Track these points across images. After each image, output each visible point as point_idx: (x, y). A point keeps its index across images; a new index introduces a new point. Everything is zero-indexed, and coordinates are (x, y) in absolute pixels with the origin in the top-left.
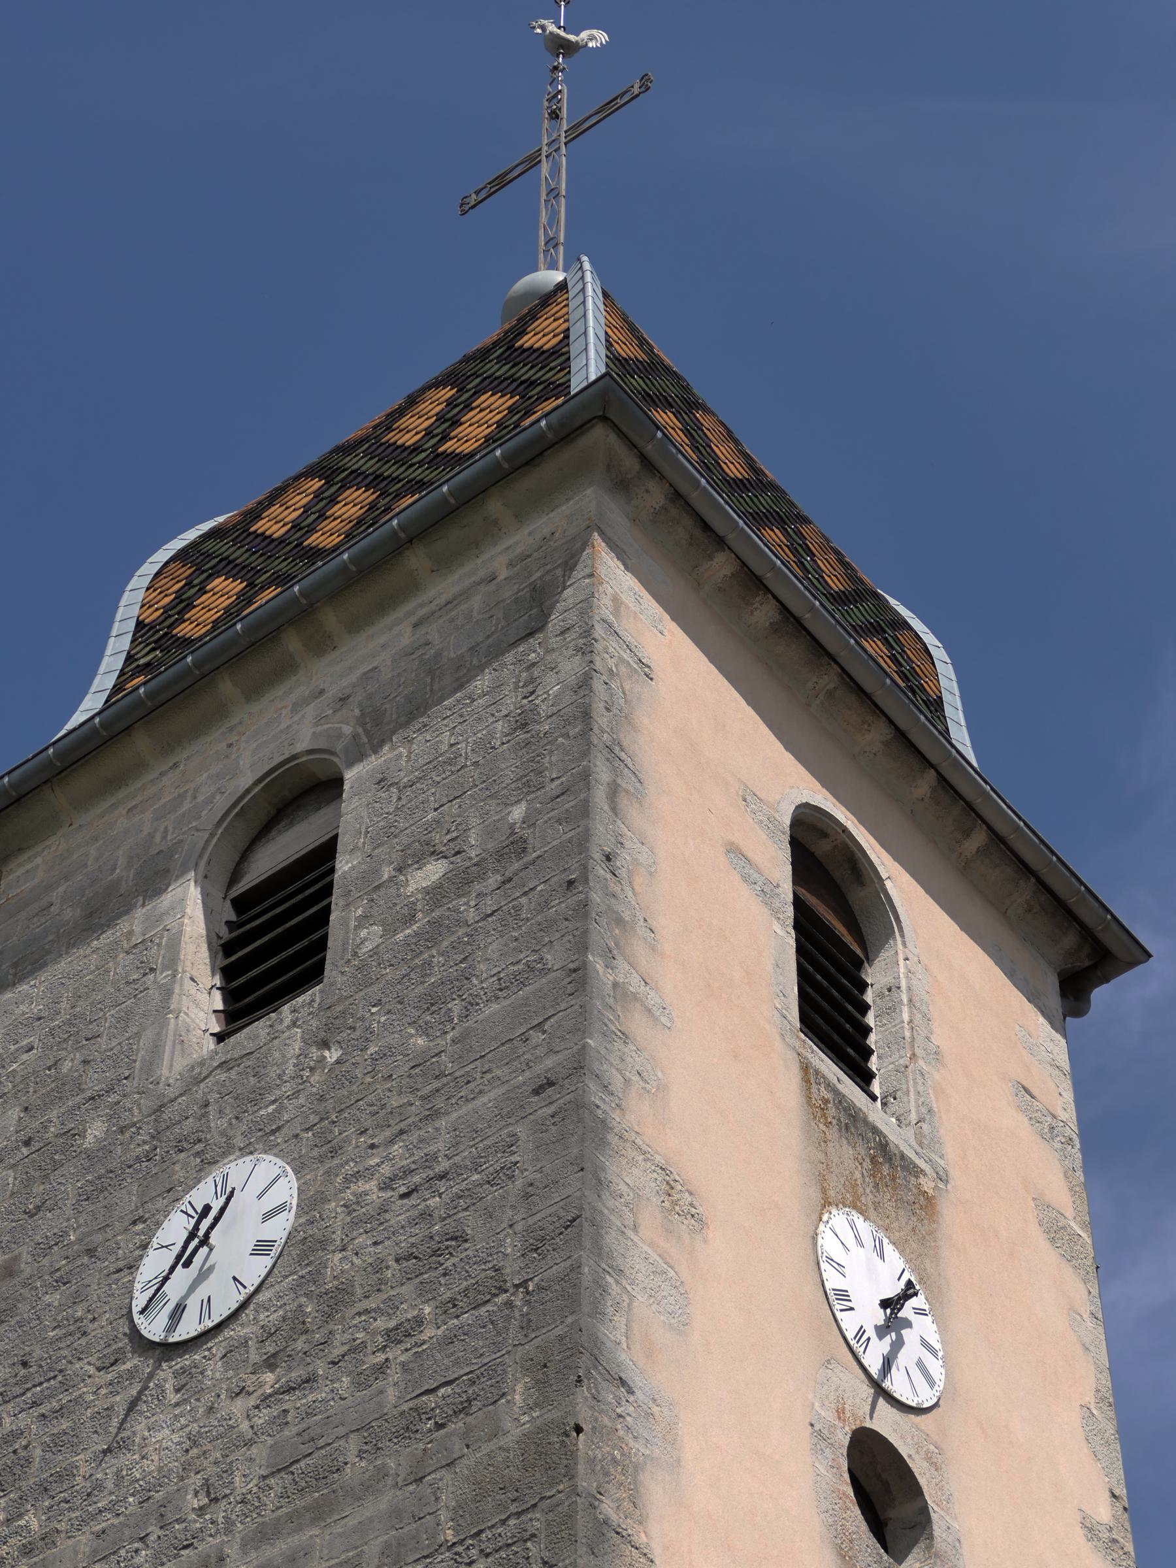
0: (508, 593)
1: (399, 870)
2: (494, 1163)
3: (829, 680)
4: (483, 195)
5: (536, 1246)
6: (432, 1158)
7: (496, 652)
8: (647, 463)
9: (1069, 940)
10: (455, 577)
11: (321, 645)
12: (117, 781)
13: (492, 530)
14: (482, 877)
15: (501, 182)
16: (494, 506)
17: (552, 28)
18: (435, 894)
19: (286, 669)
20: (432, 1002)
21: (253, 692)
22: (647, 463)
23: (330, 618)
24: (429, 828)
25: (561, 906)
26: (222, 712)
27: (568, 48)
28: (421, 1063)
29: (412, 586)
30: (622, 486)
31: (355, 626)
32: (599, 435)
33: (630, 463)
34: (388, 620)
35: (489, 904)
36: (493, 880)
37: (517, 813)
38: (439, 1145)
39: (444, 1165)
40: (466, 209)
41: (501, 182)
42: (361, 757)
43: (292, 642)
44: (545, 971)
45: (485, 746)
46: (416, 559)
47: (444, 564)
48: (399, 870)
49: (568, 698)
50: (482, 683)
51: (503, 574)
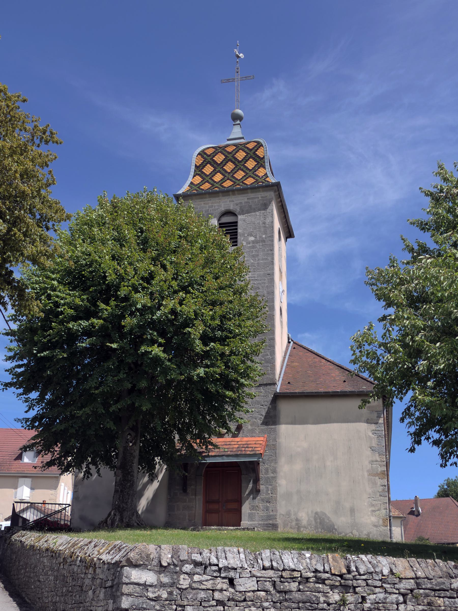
0: (261, 202)
1: (248, 236)
2: (263, 281)
3: (282, 210)
4: (225, 81)
5: (268, 293)
6: (255, 277)
7: (260, 210)
8: (278, 190)
9: (288, 235)
10: (253, 194)
11: (234, 194)
12: (202, 198)
13: (259, 191)
14: (259, 243)
15: (228, 81)
16: (261, 189)
17: (237, 53)
18: (253, 242)
19: (229, 195)
20: (253, 256)
21: (223, 196)
22: (278, 190)
23: (236, 192)
24: (252, 231)
25: (269, 252)
26: (219, 196)
27: (238, 57)
28: (252, 263)
29: (247, 193)
30: (275, 192)
31: (239, 194)
32: (276, 187)
33: (277, 190)
34: (243, 195)
35: (261, 247)
36: (261, 244)
37: (264, 236)
38: (256, 276)
39: (256, 279)
40: (222, 82)
41: (228, 81)
42: (240, 214)
43: (231, 193)
44: (268, 260)
45: (259, 223)
46: (249, 191)
47: (252, 192)
48: (248, 236)
49: (270, 223)
50: (258, 213)
51: (260, 198)
